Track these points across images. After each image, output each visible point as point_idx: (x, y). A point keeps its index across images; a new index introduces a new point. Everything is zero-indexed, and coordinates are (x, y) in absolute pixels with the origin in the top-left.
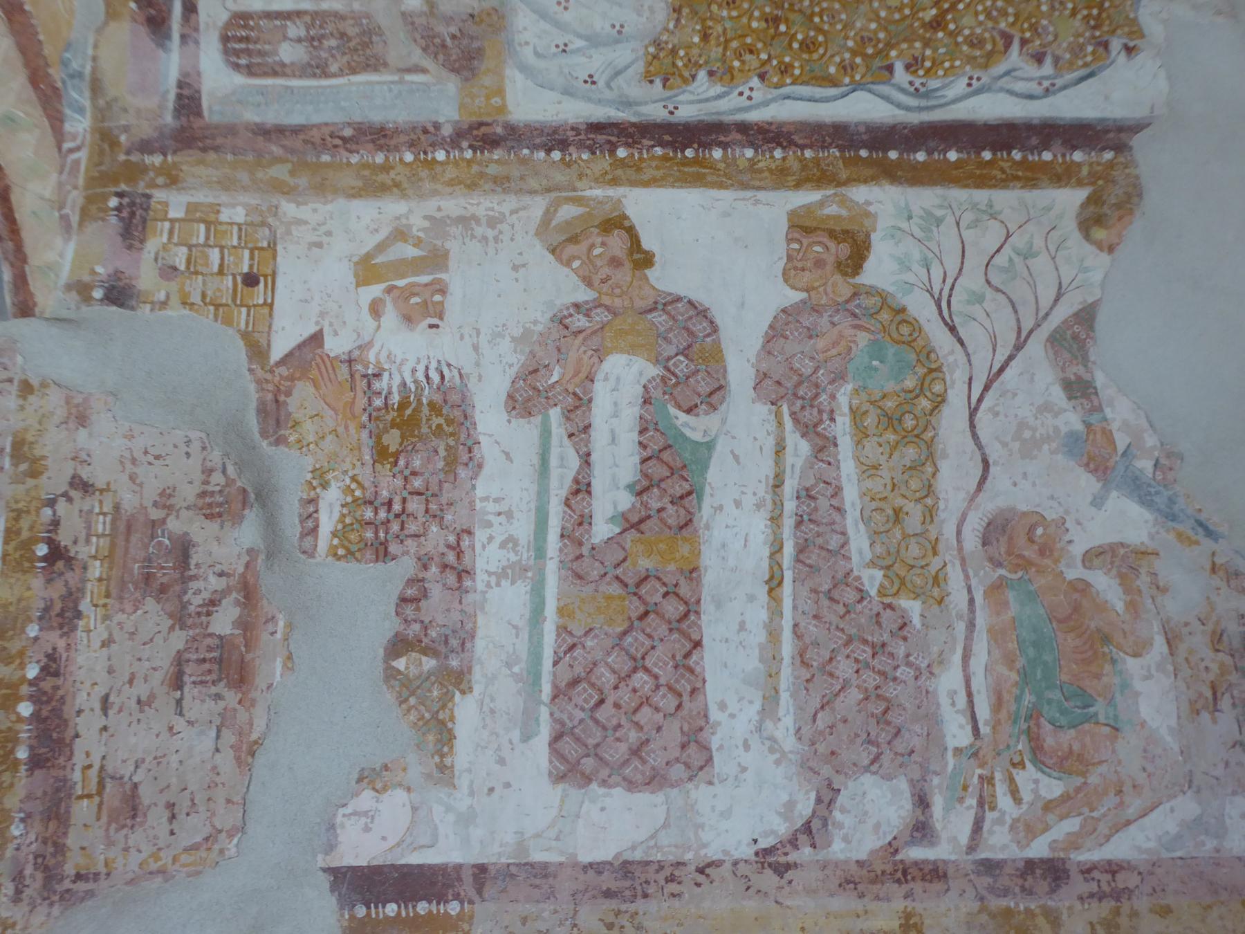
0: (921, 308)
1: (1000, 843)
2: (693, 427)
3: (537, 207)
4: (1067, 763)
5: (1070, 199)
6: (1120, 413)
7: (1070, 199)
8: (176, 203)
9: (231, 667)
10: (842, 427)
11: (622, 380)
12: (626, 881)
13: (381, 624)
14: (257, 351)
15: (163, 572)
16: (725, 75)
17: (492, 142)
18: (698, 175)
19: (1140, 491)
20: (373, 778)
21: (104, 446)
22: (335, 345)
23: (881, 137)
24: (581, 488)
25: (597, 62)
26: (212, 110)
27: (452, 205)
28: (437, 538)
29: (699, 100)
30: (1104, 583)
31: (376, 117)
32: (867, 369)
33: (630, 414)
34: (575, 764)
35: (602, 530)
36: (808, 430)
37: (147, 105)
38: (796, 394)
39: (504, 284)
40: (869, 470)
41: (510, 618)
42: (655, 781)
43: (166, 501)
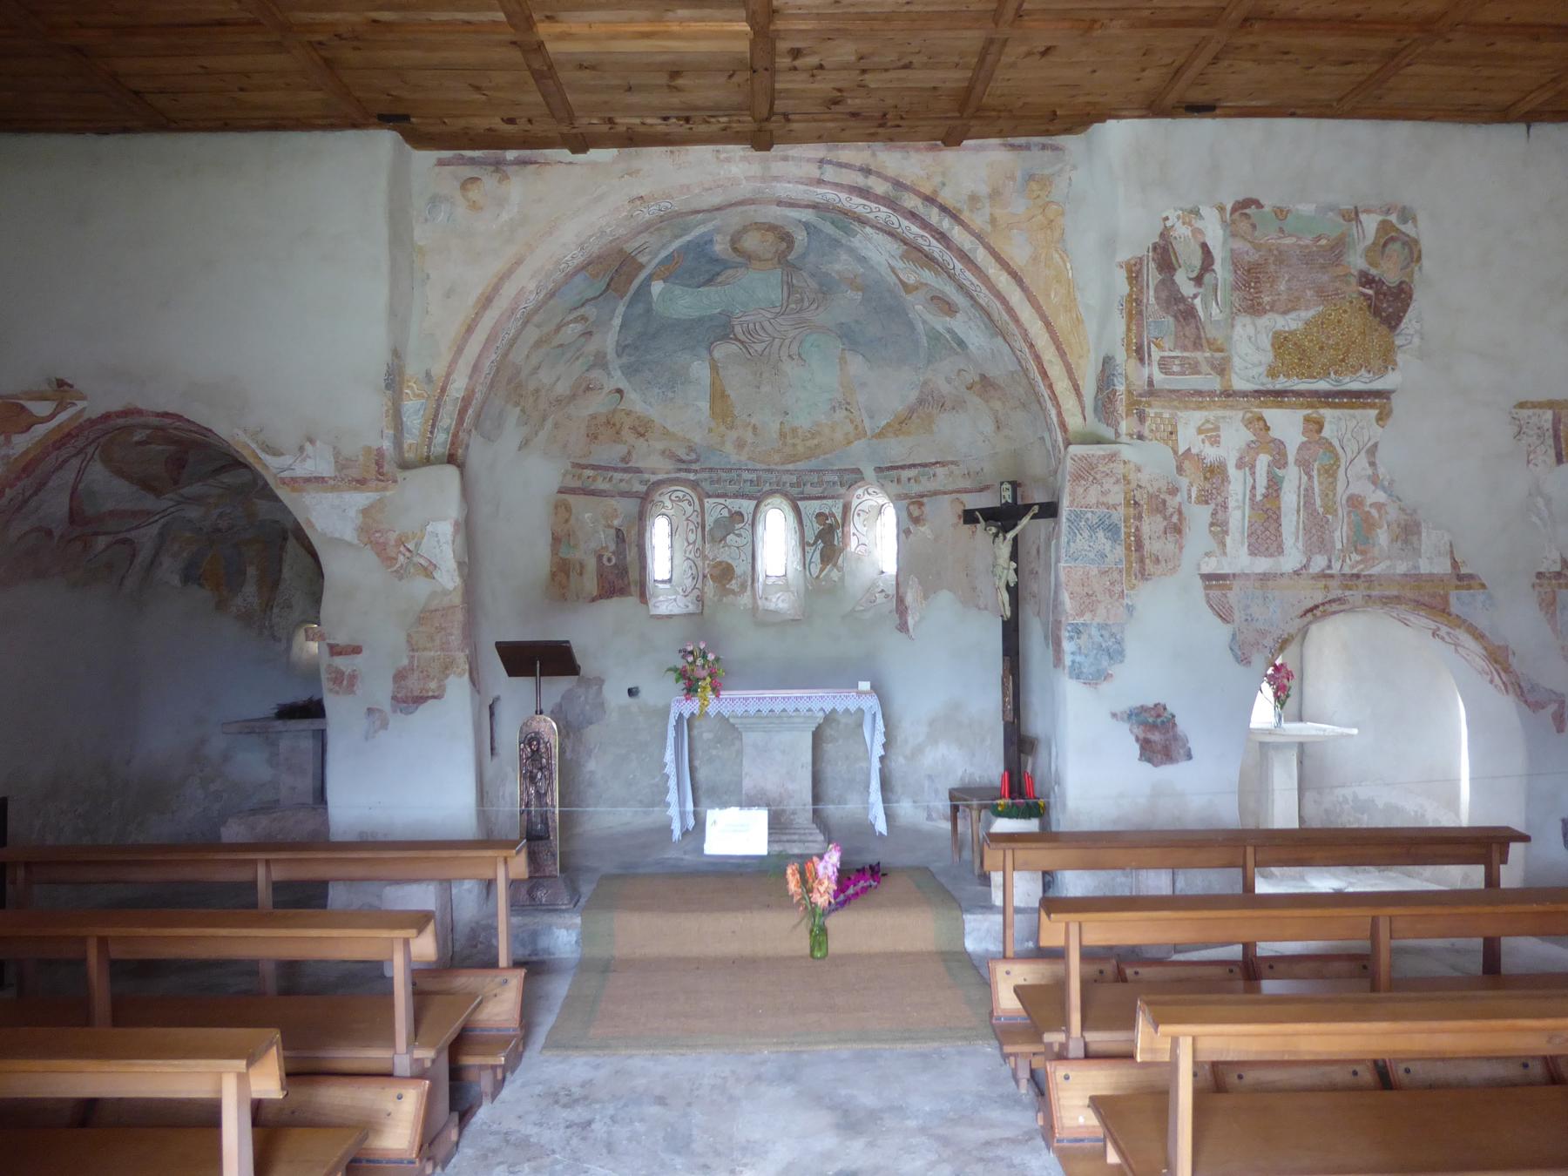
0: (1336, 443)
1: (1347, 570)
2: (1280, 472)
3: (1241, 414)
4: (1363, 553)
5: (1374, 413)
6: (1381, 470)
7: (1374, 413)
8: (1151, 412)
9: (1178, 530)
10: (1315, 473)
11: (1263, 460)
12: (1264, 578)
13: (1207, 519)
14: (1175, 452)
15: (1160, 507)
16: (1288, 376)
17: (1229, 396)
18: (1280, 406)
19: (1384, 490)
20: (1207, 554)
21: (1144, 478)
22: (1194, 451)
23: (1328, 394)
24: (1254, 487)
25: (1255, 372)
26: (1157, 386)
27: (1220, 413)
28: (1220, 499)
29: (1281, 383)
30: (1374, 512)
31: (1199, 388)
32: (1322, 457)
33: (1265, 469)
34: (1254, 552)
35: (1259, 498)
36: (1307, 474)
37: (1140, 384)
38: (1305, 465)
39: (1234, 436)
40: (1321, 483)
41: (1238, 518)
42: (1271, 555)
43: (1159, 490)
